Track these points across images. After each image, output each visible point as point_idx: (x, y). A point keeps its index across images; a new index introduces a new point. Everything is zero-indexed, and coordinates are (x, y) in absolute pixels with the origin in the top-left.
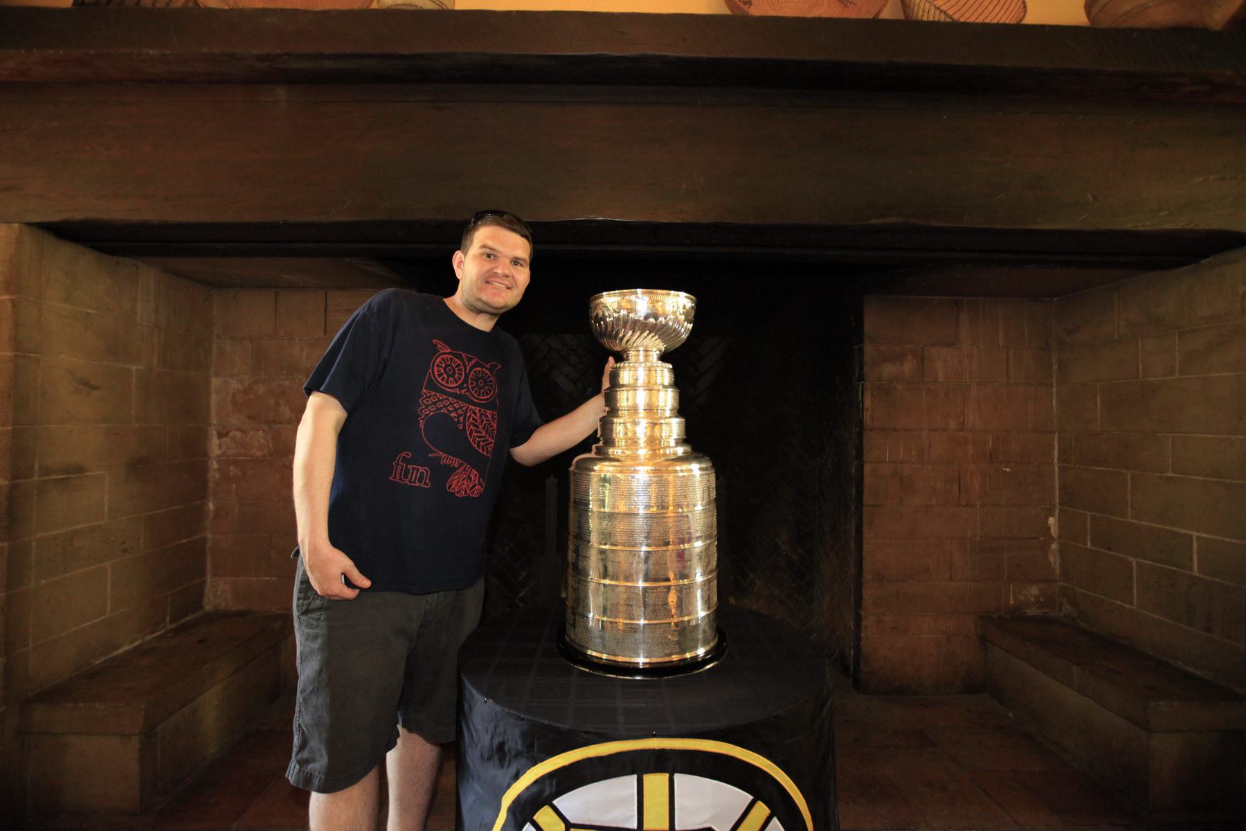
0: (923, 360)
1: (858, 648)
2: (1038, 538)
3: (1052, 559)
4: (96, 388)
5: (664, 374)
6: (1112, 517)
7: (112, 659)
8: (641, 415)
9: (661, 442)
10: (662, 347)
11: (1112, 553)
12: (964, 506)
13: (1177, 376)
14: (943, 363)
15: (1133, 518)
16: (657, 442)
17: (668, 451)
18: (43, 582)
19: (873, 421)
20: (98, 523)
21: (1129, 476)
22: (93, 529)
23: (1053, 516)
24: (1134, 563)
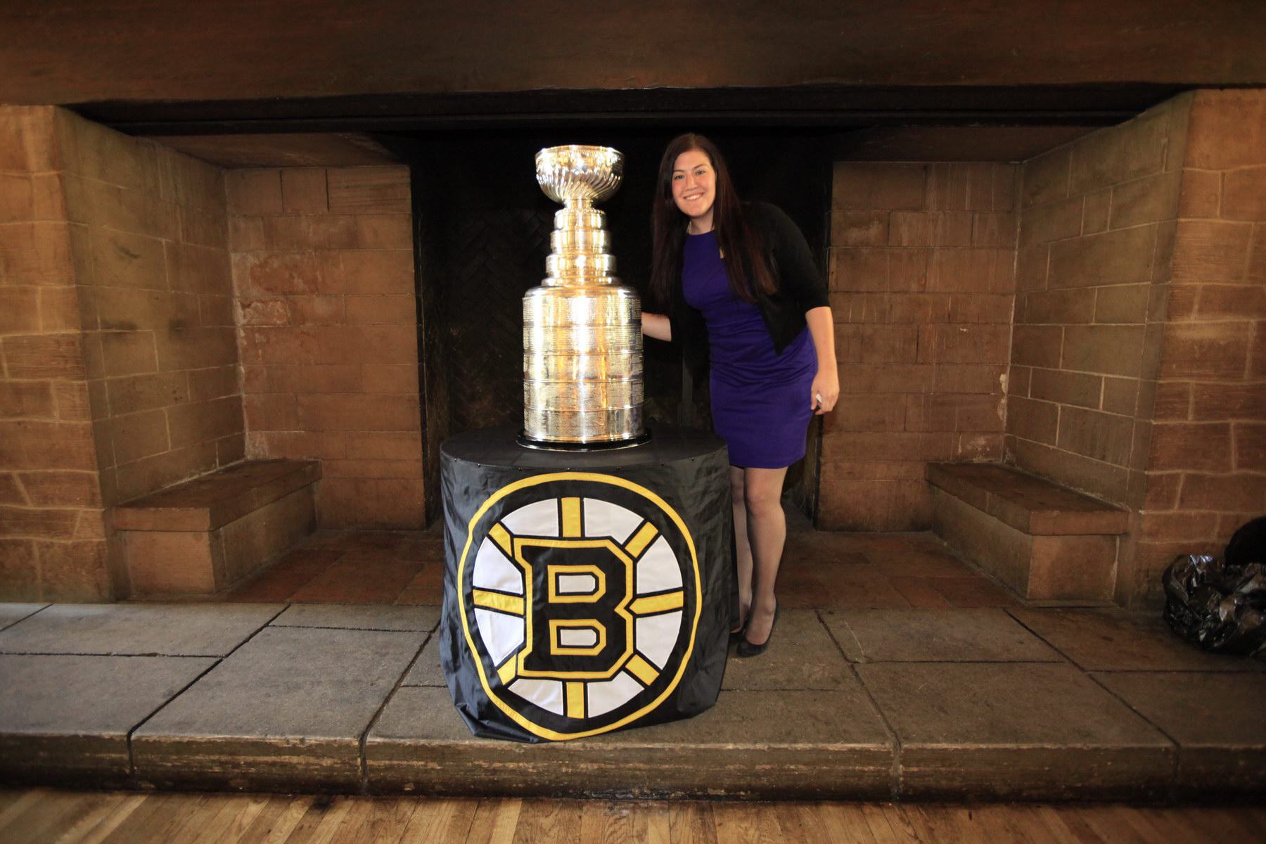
0: (889, 225)
1: (817, 491)
2: (989, 394)
3: (1000, 413)
4: (135, 257)
5: (596, 219)
6: (1049, 369)
7: (177, 486)
8: (577, 252)
9: (594, 273)
10: (596, 195)
11: (1047, 401)
12: (922, 364)
13: (1108, 230)
14: (908, 228)
15: (1062, 368)
16: (592, 273)
17: (600, 280)
18: (117, 416)
19: (837, 284)
20: (152, 373)
21: (1064, 328)
22: (150, 378)
23: (1004, 373)
24: (1060, 408)
